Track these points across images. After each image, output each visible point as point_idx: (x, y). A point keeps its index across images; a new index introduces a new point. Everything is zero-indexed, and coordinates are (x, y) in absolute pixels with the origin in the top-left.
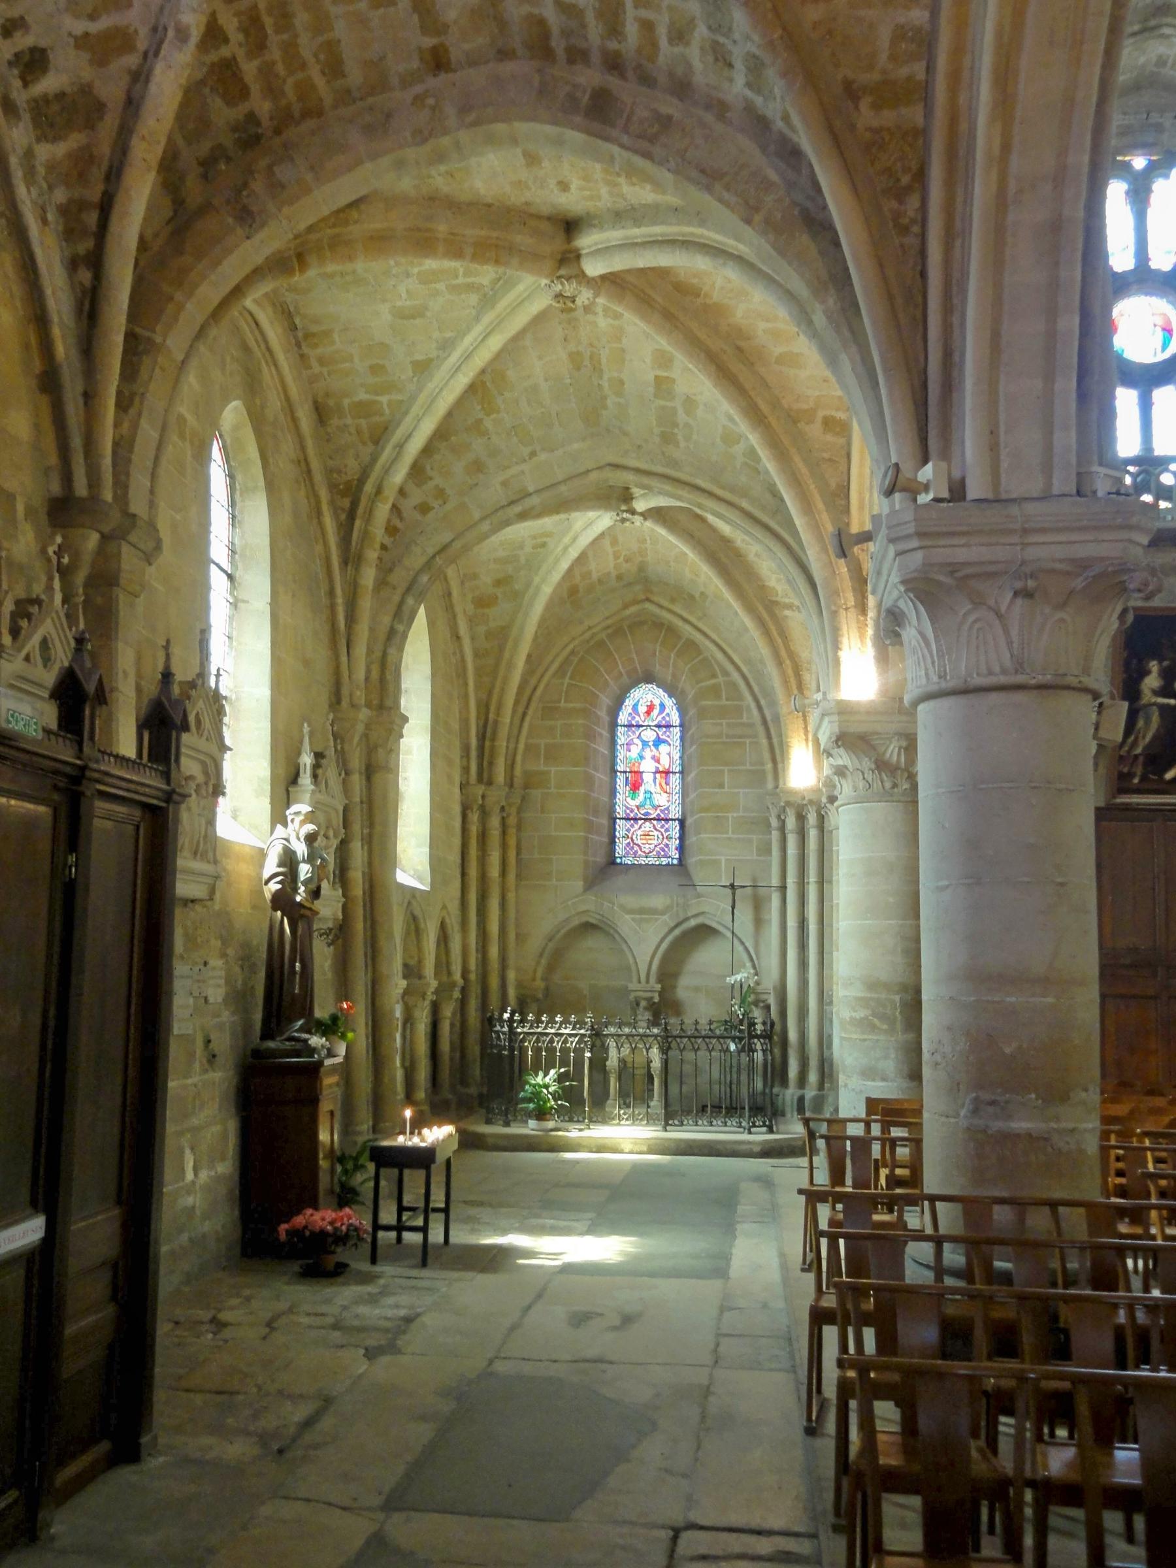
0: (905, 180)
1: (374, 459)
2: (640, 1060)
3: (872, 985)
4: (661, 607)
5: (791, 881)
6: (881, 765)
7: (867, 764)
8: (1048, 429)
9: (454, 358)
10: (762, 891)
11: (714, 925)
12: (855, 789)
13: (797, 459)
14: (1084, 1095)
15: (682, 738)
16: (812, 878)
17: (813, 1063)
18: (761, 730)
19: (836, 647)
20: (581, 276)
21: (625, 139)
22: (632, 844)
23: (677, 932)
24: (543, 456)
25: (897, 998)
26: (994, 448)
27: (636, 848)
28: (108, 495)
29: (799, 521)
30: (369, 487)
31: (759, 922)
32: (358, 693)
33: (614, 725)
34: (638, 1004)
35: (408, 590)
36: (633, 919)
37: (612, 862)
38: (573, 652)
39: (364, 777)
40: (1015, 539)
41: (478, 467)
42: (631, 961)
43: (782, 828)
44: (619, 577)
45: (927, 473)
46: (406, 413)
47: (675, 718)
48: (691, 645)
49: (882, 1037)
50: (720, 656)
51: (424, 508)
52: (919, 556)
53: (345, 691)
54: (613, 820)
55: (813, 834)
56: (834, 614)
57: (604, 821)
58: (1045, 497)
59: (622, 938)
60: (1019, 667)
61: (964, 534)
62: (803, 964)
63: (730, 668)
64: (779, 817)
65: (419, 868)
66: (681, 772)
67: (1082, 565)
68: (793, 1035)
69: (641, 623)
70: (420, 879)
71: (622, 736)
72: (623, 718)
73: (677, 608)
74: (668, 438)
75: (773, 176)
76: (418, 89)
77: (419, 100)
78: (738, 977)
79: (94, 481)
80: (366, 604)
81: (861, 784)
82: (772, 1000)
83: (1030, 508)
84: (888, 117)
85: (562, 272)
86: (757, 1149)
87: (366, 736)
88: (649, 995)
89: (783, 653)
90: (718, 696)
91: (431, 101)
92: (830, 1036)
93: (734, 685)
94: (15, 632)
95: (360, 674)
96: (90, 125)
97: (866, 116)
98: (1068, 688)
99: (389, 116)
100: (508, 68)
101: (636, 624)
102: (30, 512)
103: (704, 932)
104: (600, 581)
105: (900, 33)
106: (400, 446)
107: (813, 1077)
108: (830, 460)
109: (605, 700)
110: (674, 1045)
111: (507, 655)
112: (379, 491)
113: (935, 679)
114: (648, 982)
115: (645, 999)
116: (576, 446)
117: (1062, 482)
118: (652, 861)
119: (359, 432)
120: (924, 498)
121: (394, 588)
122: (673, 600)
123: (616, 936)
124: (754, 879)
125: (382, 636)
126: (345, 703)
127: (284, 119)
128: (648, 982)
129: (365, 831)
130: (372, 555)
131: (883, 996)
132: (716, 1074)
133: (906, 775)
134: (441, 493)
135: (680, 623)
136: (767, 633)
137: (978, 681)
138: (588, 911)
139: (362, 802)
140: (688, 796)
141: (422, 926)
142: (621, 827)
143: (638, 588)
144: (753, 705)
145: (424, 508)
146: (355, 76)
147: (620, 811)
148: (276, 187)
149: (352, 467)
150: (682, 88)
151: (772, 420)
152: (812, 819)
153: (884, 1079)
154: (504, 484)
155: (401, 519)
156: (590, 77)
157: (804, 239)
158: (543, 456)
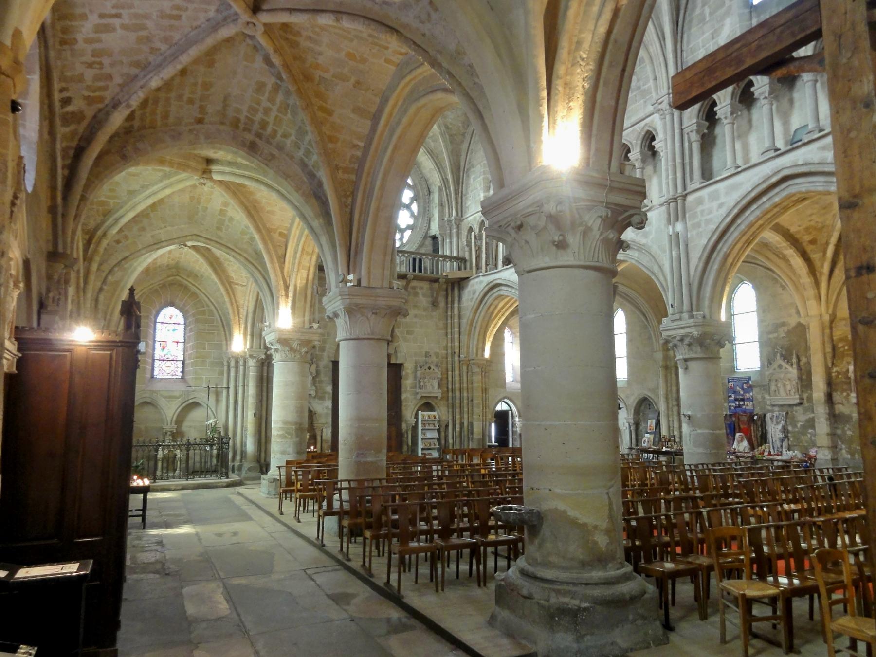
0: (348, 193)
1: (103, 222)
2: (171, 455)
3: (285, 423)
4: (183, 278)
5: (232, 386)
6: (291, 349)
7: (287, 349)
9: (147, 193)
10: (219, 389)
11: (200, 402)
12: (282, 356)
13: (270, 245)
15: (185, 329)
16: (241, 385)
17: (239, 452)
18: (222, 329)
19: (278, 309)
20: (211, 179)
21: (260, 158)
22: (161, 370)
23: (184, 405)
24: (169, 228)
26: (369, 273)
29: (268, 265)
30: (100, 233)
31: (217, 401)
33: (155, 322)
34: (166, 433)
37: (152, 377)
38: (143, 293)
40: (373, 298)
43: (229, 366)
44: (168, 265)
45: (351, 277)
46: (122, 207)
47: (182, 321)
48: (194, 295)
50: (206, 299)
52: (348, 301)
54: (154, 360)
55: (241, 368)
56: (278, 298)
57: (150, 360)
58: (382, 288)
60: (372, 334)
62: (235, 416)
63: (210, 304)
64: (228, 362)
66: (184, 342)
67: (390, 307)
69: (174, 284)
71: (158, 326)
72: (159, 319)
73: (189, 280)
74: (219, 228)
75: (305, 179)
76: (191, 127)
77: (190, 130)
78: (211, 422)
80: (92, 277)
81: (284, 355)
82: (222, 430)
83: (378, 290)
84: (346, 176)
85: (205, 176)
86: (225, 484)
89: (234, 301)
90: (205, 315)
91: (195, 132)
92: (246, 443)
93: (211, 311)
96: (79, 123)
97: (340, 175)
99: (180, 134)
100: (222, 127)
101: (172, 284)
103: (196, 405)
104: (159, 266)
105: (353, 156)
106: (117, 220)
107: (238, 458)
109: (154, 312)
110: (192, 448)
111: (117, 293)
112: (104, 235)
113: (348, 334)
116: (183, 226)
117: (386, 284)
118: (171, 377)
119: (98, 211)
120: (349, 284)
122: (188, 276)
124: (216, 385)
125: (97, 290)
127: (143, 127)
130: (97, 259)
132: (197, 459)
134: (126, 237)
135: (191, 285)
136: (228, 293)
140: (187, 351)
142: (157, 363)
143: (174, 270)
144: (219, 319)
146: (171, 119)
147: (157, 356)
148: (137, 150)
149: (92, 224)
150: (280, 148)
151: (263, 231)
152: (241, 363)
154: (152, 236)
156: (249, 137)
157: (314, 200)
158: (169, 228)
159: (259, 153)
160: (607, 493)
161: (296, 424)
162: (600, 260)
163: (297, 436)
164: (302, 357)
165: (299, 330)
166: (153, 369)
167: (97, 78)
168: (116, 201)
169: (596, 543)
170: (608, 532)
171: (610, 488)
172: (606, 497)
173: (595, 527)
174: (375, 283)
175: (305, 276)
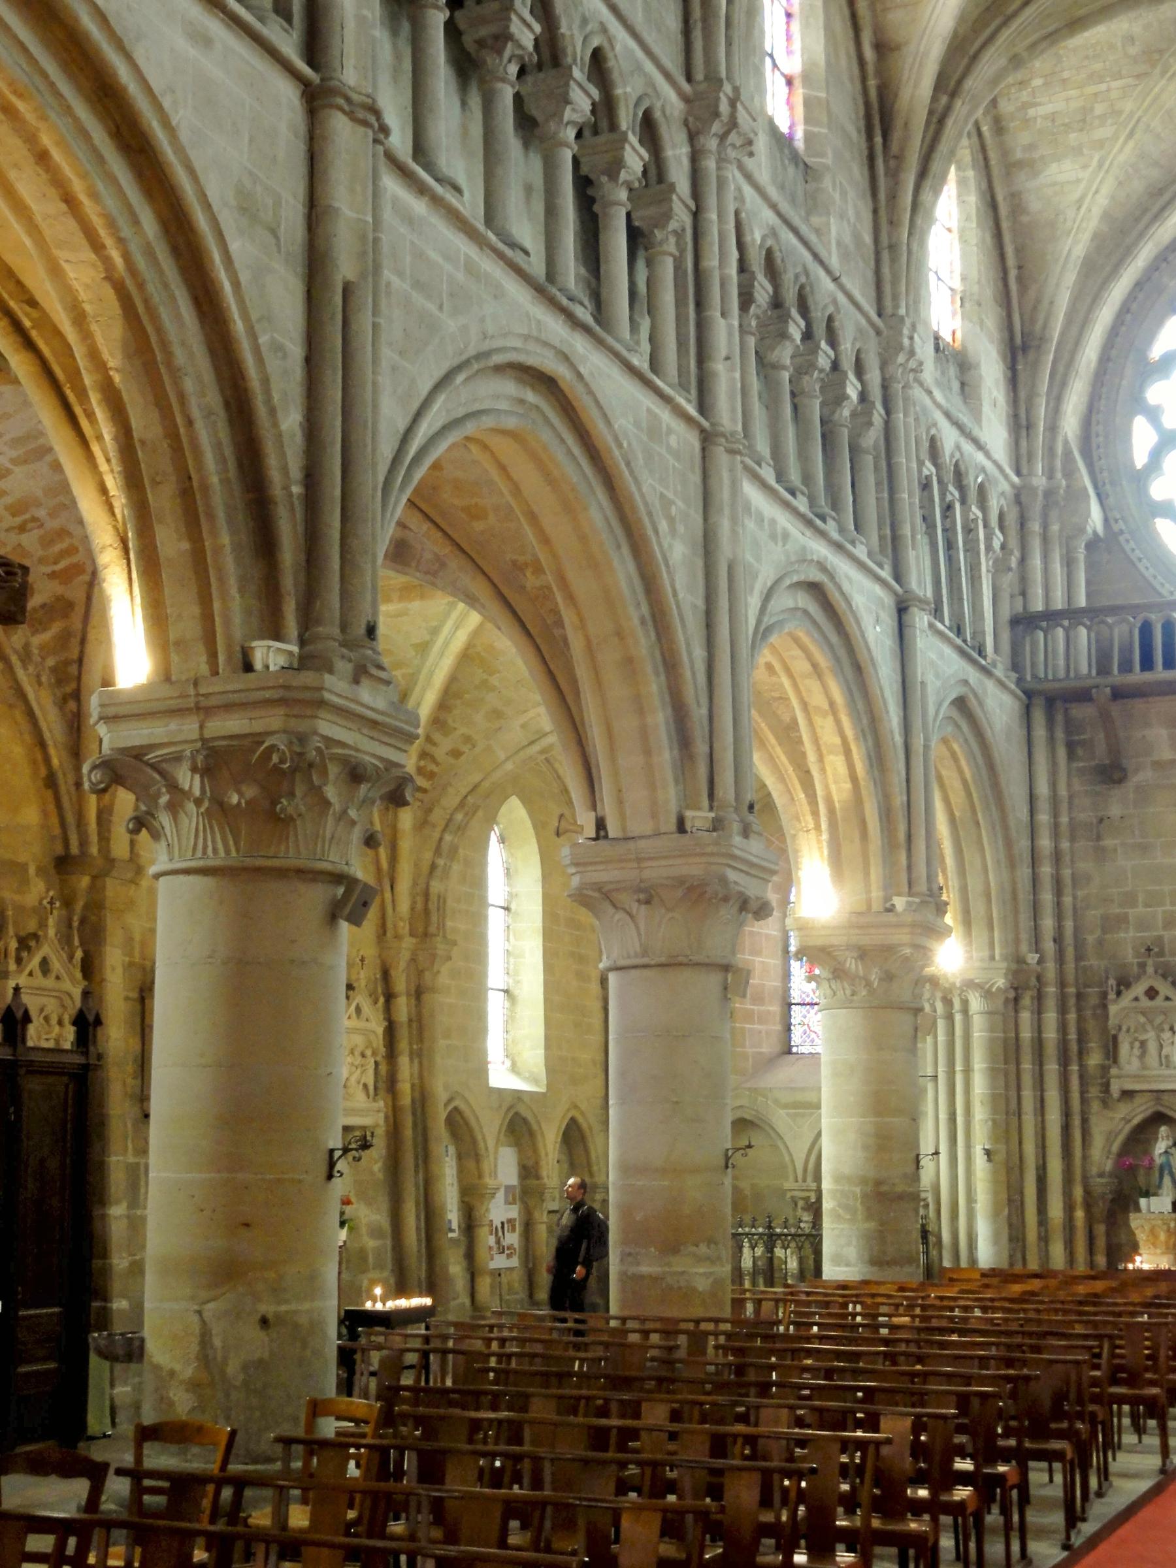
8: (652, 786)
14: (694, 1249)
21: (418, 574)
25: (858, 1190)
26: (620, 802)
27: (813, 1035)
28: (94, 850)
32: (402, 924)
35: (447, 826)
36: (788, 1114)
37: (789, 1052)
39: (413, 1001)
41: (497, 714)
42: (787, 1159)
49: (846, 1226)
51: (456, 754)
53: (389, 925)
54: (790, 1004)
55: (958, 1018)
57: (775, 1008)
58: (657, 834)
59: (779, 1135)
60: (645, 953)
61: (602, 863)
65: (535, 1070)
67: (681, 881)
68: (946, 1236)
70: (536, 1081)
79: (84, 843)
83: (642, 844)
87: (413, 960)
88: (806, 1194)
94: (19, 960)
95: (404, 906)
96: (66, 616)
98: (681, 964)
102: (40, 871)
108: (781, 698)
114: (804, 1180)
115: (802, 1199)
121: (434, 826)
123: (771, 1132)
126: (389, 934)
128: (804, 1180)
129: (415, 1047)
131: (847, 1188)
133: (864, 983)
134: (467, 739)
137: (622, 962)
138: (741, 1107)
139: (410, 1020)
141: (535, 1127)
142: (797, 1013)
145: (456, 754)
147: (795, 996)
153: (847, 1265)
154: (523, 726)
155: (437, 764)
159: (414, 564)
160: (199, 1313)
161: (863, 1181)
162: (199, 854)
163: (869, 1216)
164: (872, 991)
165: (860, 920)
166: (788, 1029)
167: (47, 541)
168: (404, 671)
169: (171, 1404)
170: (194, 1386)
171: (204, 1303)
172: (195, 1319)
173: (172, 1373)
174: (640, 825)
175: (842, 770)
